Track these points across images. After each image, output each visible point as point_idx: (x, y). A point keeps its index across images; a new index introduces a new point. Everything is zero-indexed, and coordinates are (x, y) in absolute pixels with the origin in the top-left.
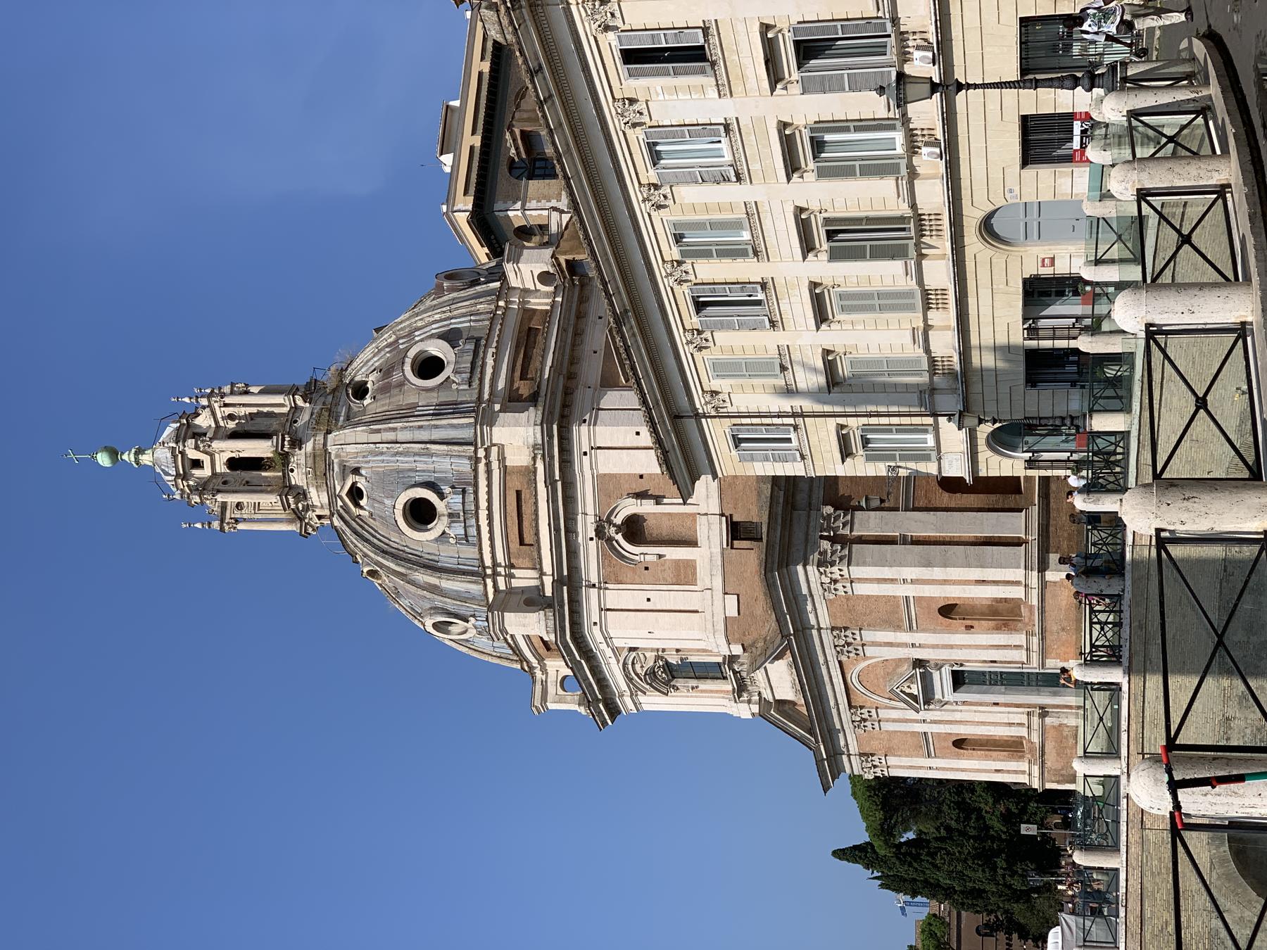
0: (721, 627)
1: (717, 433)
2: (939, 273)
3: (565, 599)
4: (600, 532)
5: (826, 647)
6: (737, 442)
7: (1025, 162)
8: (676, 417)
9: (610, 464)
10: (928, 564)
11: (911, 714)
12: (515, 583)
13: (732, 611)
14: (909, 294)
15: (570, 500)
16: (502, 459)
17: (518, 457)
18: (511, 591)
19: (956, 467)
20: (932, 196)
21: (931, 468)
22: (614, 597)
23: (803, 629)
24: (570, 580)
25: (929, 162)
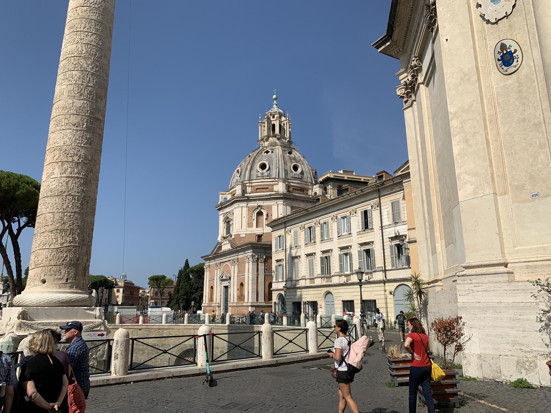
0: (238, 233)
1: (281, 232)
2: (318, 282)
3: (244, 198)
4: (259, 206)
6: (280, 236)
7: (343, 301)
8: (285, 223)
9: (274, 208)
10: (252, 280)
11: (218, 276)
12: (248, 187)
14: (313, 275)
15: (266, 199)
16: (275, 184)
17: (276, 188)
18: (246, 187)
19: (274, 286)
20: (335, 280)
21: (274, 280)
22: (245, 210)
23: (238, 252)
24: (248, 200)
25: (343, 280)
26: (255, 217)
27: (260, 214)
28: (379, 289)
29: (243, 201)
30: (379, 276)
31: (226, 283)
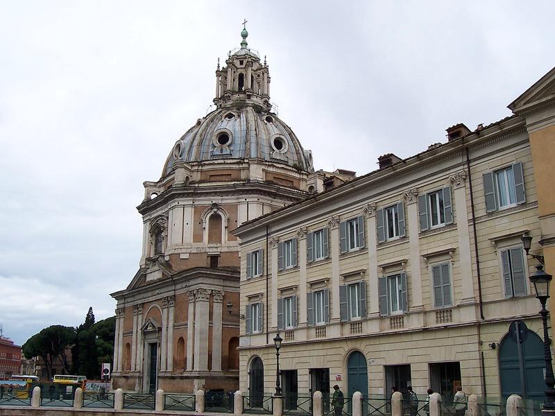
0: (176, 252)
1: (260, 244)
2: (333, 333)
4: (215, 205)
5: (167, 293)
6: (255, 253)
7: (386, 367)
8: (267, 226)
9: (242, 210)
10: (201, 333)
11: (140, 327)
13: (182, 256)
14: (448, 301)
15: (227, 193)
16: (244, 169)
19: (243, 342)
20: (372, 328)
21: (242, 331)
22: (189, 212)
23: (174, 283)
25: (313, 336)
26: (206, 225)
27: (216, 218)
28: (465, 340)
29: (188, 195)
30: (469, 316)
31: (152, 339)
